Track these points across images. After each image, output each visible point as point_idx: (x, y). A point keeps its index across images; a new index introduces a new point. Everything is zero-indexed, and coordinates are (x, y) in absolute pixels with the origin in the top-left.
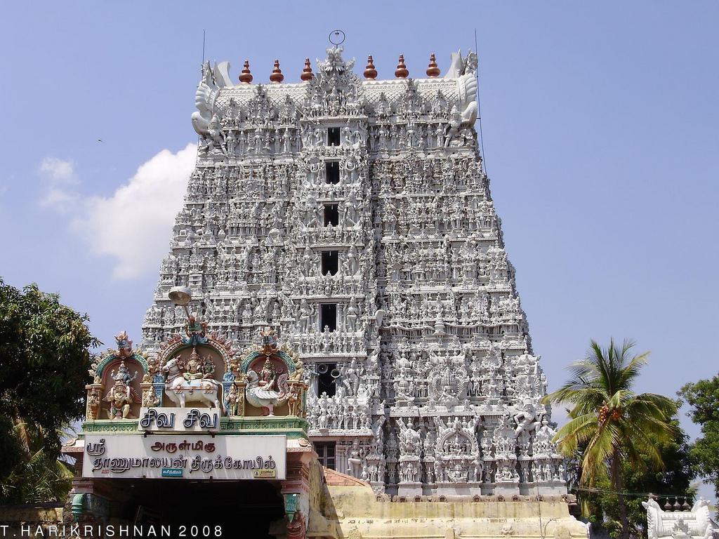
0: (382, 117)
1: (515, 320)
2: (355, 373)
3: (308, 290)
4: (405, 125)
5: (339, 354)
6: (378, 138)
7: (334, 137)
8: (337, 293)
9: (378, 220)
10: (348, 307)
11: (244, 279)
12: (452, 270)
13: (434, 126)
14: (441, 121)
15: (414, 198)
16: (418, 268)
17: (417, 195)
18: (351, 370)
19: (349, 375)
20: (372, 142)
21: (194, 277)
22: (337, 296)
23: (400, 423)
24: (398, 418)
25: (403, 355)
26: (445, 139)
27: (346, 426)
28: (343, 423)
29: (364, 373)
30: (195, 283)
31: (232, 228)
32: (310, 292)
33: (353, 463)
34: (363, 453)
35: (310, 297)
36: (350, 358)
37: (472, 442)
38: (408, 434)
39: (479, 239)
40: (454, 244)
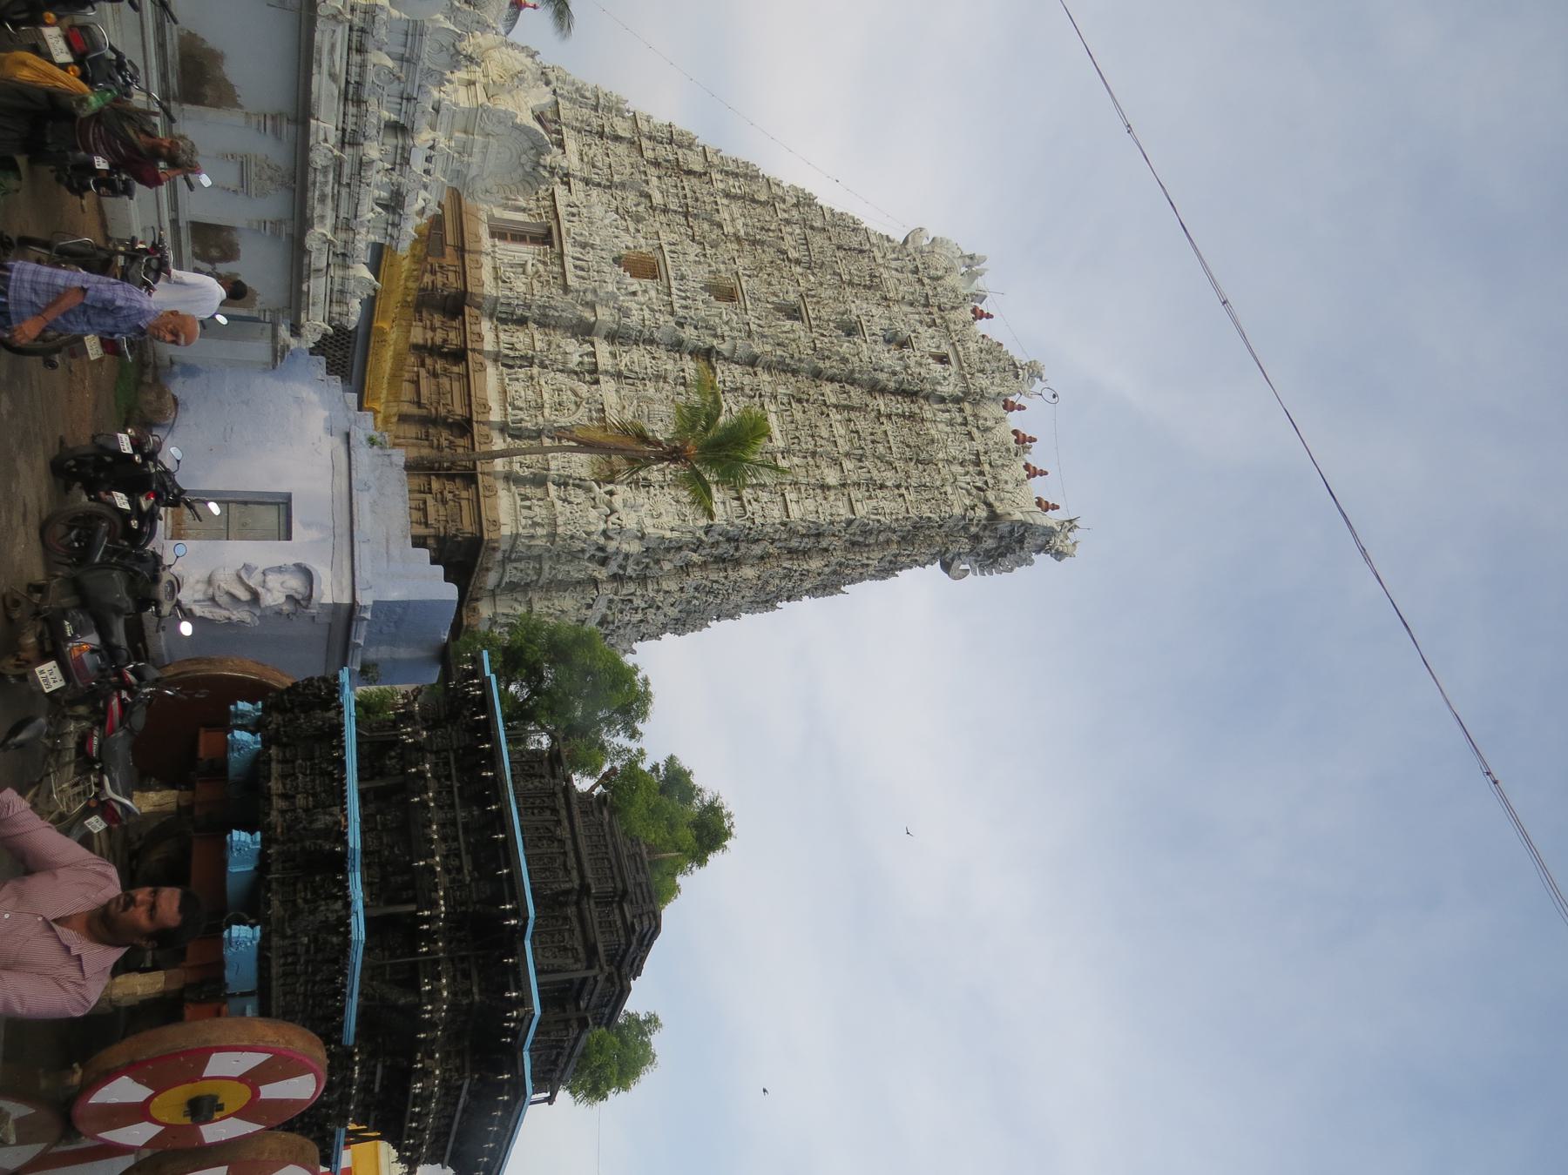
0: (975, 416)
1: (753, 514)
2: (650, 299)
3: (749, 276)
4: (973, 439)
5: (674, 283)
6: (948, 411)
7: (942, 359)
8: (752, 304)
9: (847, 387)
10: (736, 314)
11: (747, 234)
12: (806, 457)
13: (981, 473)
14: (991, 482)
15: (885, 432)
16: (799, 416)
17: (891, 439)
18: (653, 293)
19: (645, 291)
20: (942, 406)
21: (740, 187)
22: (748, 303)
23: (587, 348)
24: (593, 347)
25: (682, 374)
26: (969, 484)
27: (578, 263)
28: (579, 259)
29: (652, 310)
30: (734, 187)
31: (806, 239)
32: (746, 278)
33: (523, 266)
34: (540, 276)
35: (740, 274)
36: (670, 295)
37: (571, 419)
38: (574, 351)
39: (852, 496)
40: (838, 467)
